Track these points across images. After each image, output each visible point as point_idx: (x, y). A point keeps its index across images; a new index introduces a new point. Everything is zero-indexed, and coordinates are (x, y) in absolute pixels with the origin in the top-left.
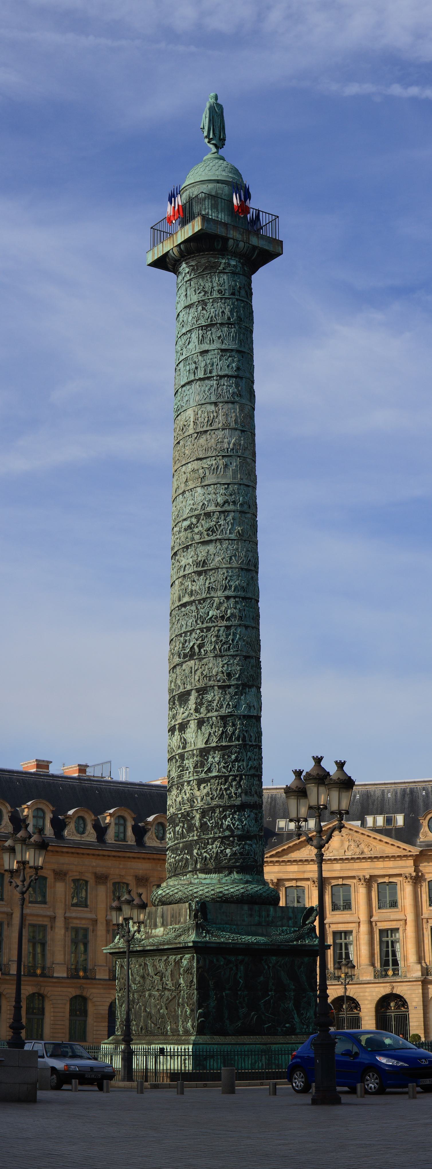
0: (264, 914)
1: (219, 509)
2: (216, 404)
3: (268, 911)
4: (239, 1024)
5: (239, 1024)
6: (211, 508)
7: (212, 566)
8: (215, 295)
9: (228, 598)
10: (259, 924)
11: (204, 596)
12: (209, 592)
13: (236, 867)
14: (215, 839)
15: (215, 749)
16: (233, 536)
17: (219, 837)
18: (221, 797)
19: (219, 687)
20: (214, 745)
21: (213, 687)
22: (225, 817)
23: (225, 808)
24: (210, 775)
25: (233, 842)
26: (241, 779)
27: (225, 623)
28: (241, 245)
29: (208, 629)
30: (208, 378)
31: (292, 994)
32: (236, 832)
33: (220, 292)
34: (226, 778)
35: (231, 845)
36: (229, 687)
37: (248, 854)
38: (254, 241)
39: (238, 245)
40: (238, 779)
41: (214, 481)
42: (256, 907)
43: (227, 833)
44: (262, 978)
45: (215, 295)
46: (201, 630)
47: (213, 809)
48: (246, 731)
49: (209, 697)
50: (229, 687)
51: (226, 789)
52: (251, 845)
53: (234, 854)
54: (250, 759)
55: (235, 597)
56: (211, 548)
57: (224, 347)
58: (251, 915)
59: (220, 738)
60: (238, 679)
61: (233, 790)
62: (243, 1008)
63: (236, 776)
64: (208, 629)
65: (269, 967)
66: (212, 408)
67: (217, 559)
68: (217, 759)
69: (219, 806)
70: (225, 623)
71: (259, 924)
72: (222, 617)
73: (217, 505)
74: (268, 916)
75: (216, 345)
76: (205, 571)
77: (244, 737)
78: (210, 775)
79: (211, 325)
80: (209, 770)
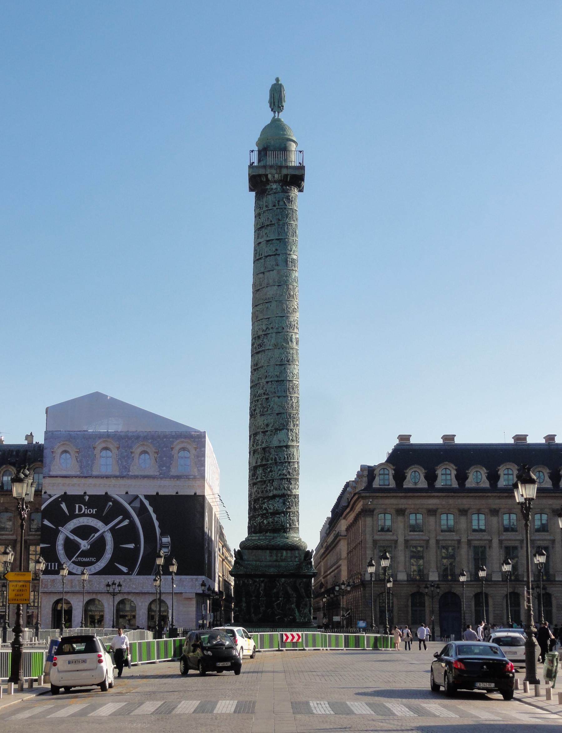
0: (279, 555)
1: (264, 333)
2: (263, 273)
3: (282, 553)
4: (260, 616)
5: (260, 616)
6: (260, 333)
7: (260, 365)
8: (265, 209)
9: (267, 382)
10: (276, 561)
11: (256, 383)
12: (258, 380)
13: (269, 530)
14: (259, 515)
15: (260, 466)
16: (270, 348)
17: (261, 514)
18: (262, 492)
19: (262, 432)
20: (259, 464)
21: (259, 432)
22: (264, 503)
23: (264, 498)
24: (258, 480)
25: (267, 516)
26: (273, 481)
27: (266, 397)
28: (276, 176)
29: (258, 401)
30: (260, 259)
31: (295, 599)
32: (270, 511)
33: (267, 206)
34: (265, 482)
35: (267, 518)
36: (267, 431)
37: (277, 522)
38: (285, 172)
39: (274, 177)
40: (271, 482)
41: (262, 318)
42: (275, 552)
43: (265, 512)
44: (275, 590)
45: (265, 209)
46: (255, 401)
47: (258, 499)
48: (277, 455)
49: (257, 438)
50: (267, 431)
51: (265, 488)
52: (279, 517)
53: (269, 523)
54: (279, 470)
55: (271, 381)
56: (259, 355)
57: (268, 239)
58: (271, 556)
59: (262, 460)
60: (272, 427)
61: (268, 488)
62: (263, 607)
63: (270, 480)
64: (258, 401)
65: (280, 584)
66: (261, 275)
67: (263, 361)
68: (261, 472)
69: (261, 497)
70: (266, 397)
71: (276, 561)
72: (264, 394)
73: (263, 331)
74: (282, 556)
75: (265, 238)
76: (257, 369)
77: (276, 458)
78: (258, 480)
79: (262, 227)
80: (257, 478)
